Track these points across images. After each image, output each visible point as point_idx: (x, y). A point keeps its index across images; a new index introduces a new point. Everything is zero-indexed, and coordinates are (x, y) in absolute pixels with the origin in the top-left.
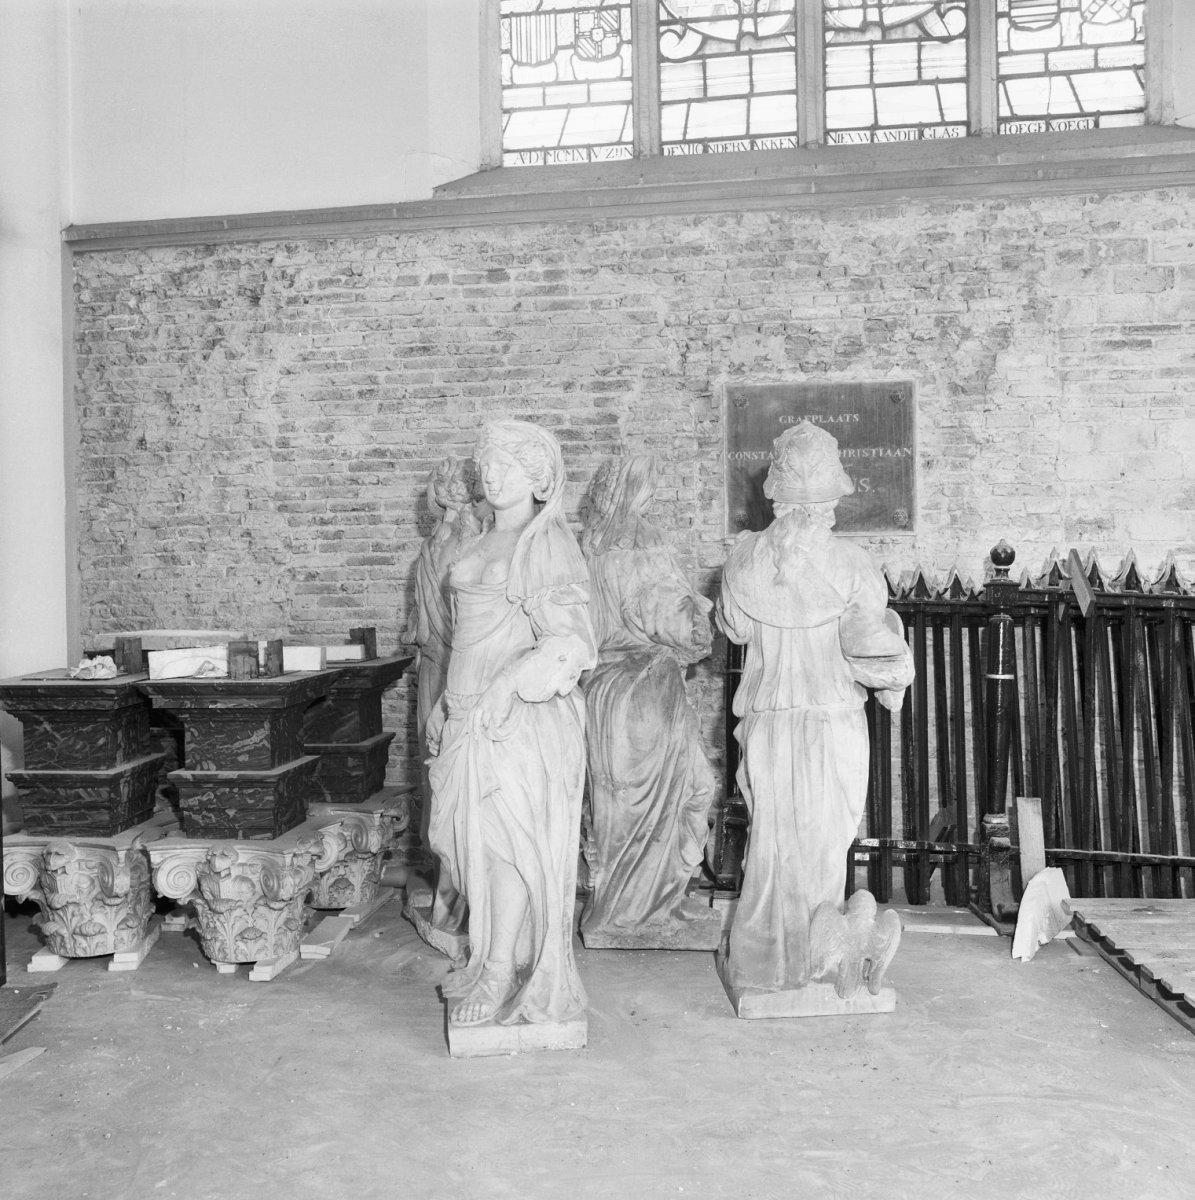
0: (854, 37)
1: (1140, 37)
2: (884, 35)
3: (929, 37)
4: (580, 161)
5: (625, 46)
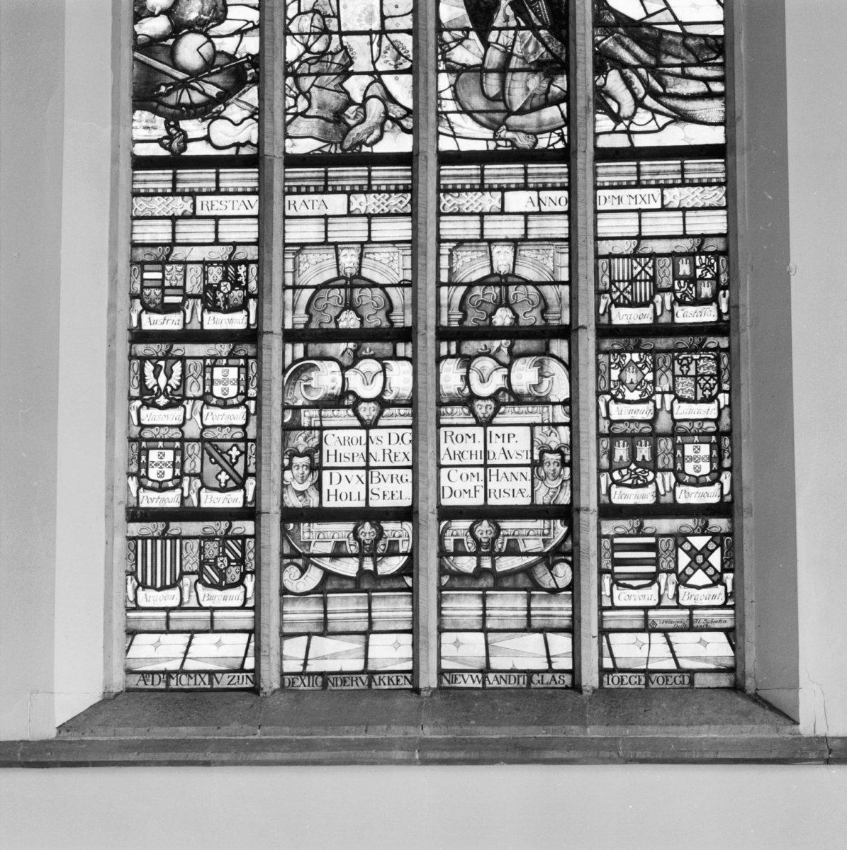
0: (467, 582)
1: (730, 603)
2: (495, 583)
3: (539, 588)
4: (202, 686)
5: (249, 576)
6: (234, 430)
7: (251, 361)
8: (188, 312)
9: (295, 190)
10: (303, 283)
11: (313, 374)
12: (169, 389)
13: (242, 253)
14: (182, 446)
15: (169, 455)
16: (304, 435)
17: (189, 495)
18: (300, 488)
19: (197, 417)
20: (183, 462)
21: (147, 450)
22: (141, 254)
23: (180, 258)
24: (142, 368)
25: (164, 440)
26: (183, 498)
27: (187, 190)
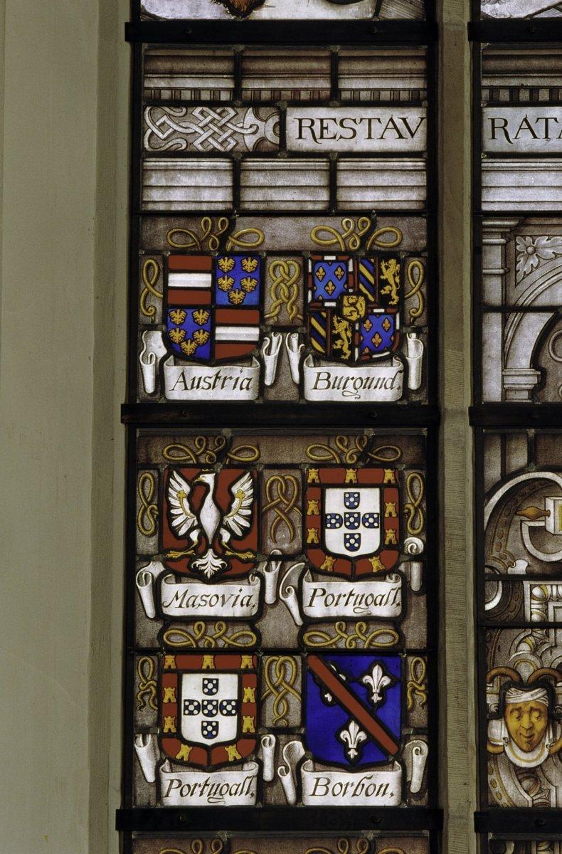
6: (376, 629)
7: (409, 475)
8: (270, 362)
9: (505, 96)
10: (525, 300)
11: (550, 503)
12: (226, 536)
13: (389, 233)
14: (259, 664)
15: (228, 687)
16: (531, 640)
17: (276, 778)
18: (524, 760)
19: (291, 600)
20: (260, 703)
21: (178, 674)
22: (160, 235)
23: (250, 243)
24: (162, 491)
25: (215, 652)
26: (262, 786)
27: (266, 96)
